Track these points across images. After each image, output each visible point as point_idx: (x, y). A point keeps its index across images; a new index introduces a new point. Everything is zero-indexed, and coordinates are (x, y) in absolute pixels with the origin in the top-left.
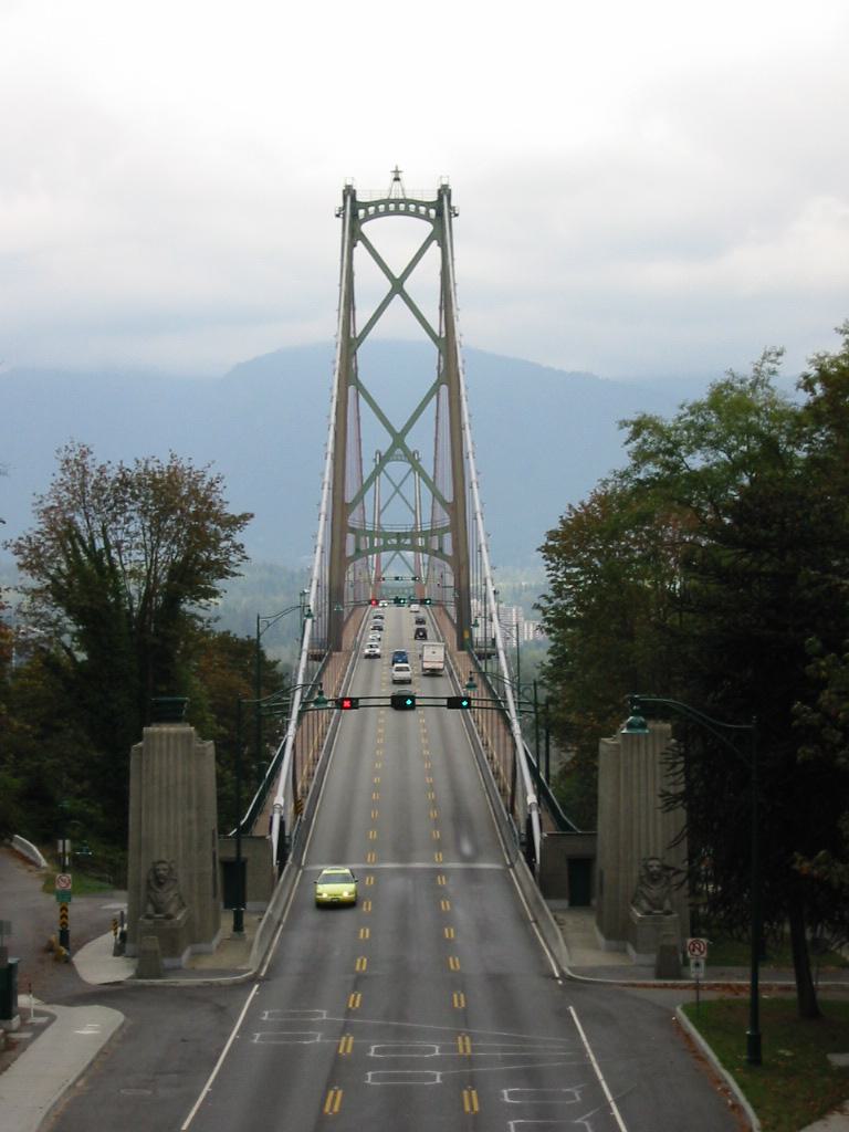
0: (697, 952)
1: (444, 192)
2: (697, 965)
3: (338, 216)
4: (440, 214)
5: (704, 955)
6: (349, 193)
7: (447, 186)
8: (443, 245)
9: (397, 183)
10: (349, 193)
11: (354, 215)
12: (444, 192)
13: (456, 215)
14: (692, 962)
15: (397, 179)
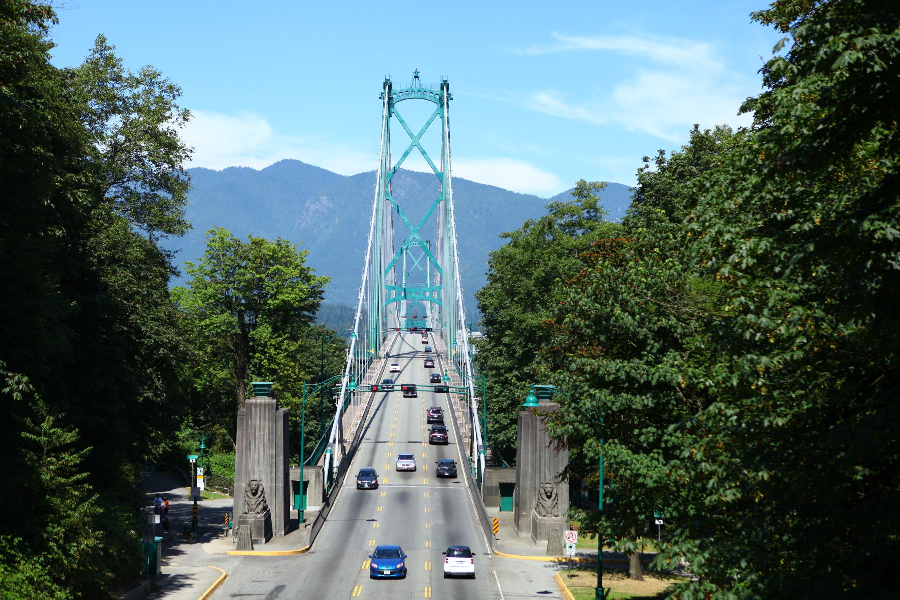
0: (571, 540)
1: (445, 86)
2: (571, 547)
3: (380, 98)
4: (441, 99)
5: (576, 542)
6: (388, 85)
7: (447, 81)
8: (442, 118)
9: (416, 81)
10: (388, 85)
11: (390, 99)
12: (445, 86)
13: (452, 99)
14: (568, 545)
15: (417, 77)
